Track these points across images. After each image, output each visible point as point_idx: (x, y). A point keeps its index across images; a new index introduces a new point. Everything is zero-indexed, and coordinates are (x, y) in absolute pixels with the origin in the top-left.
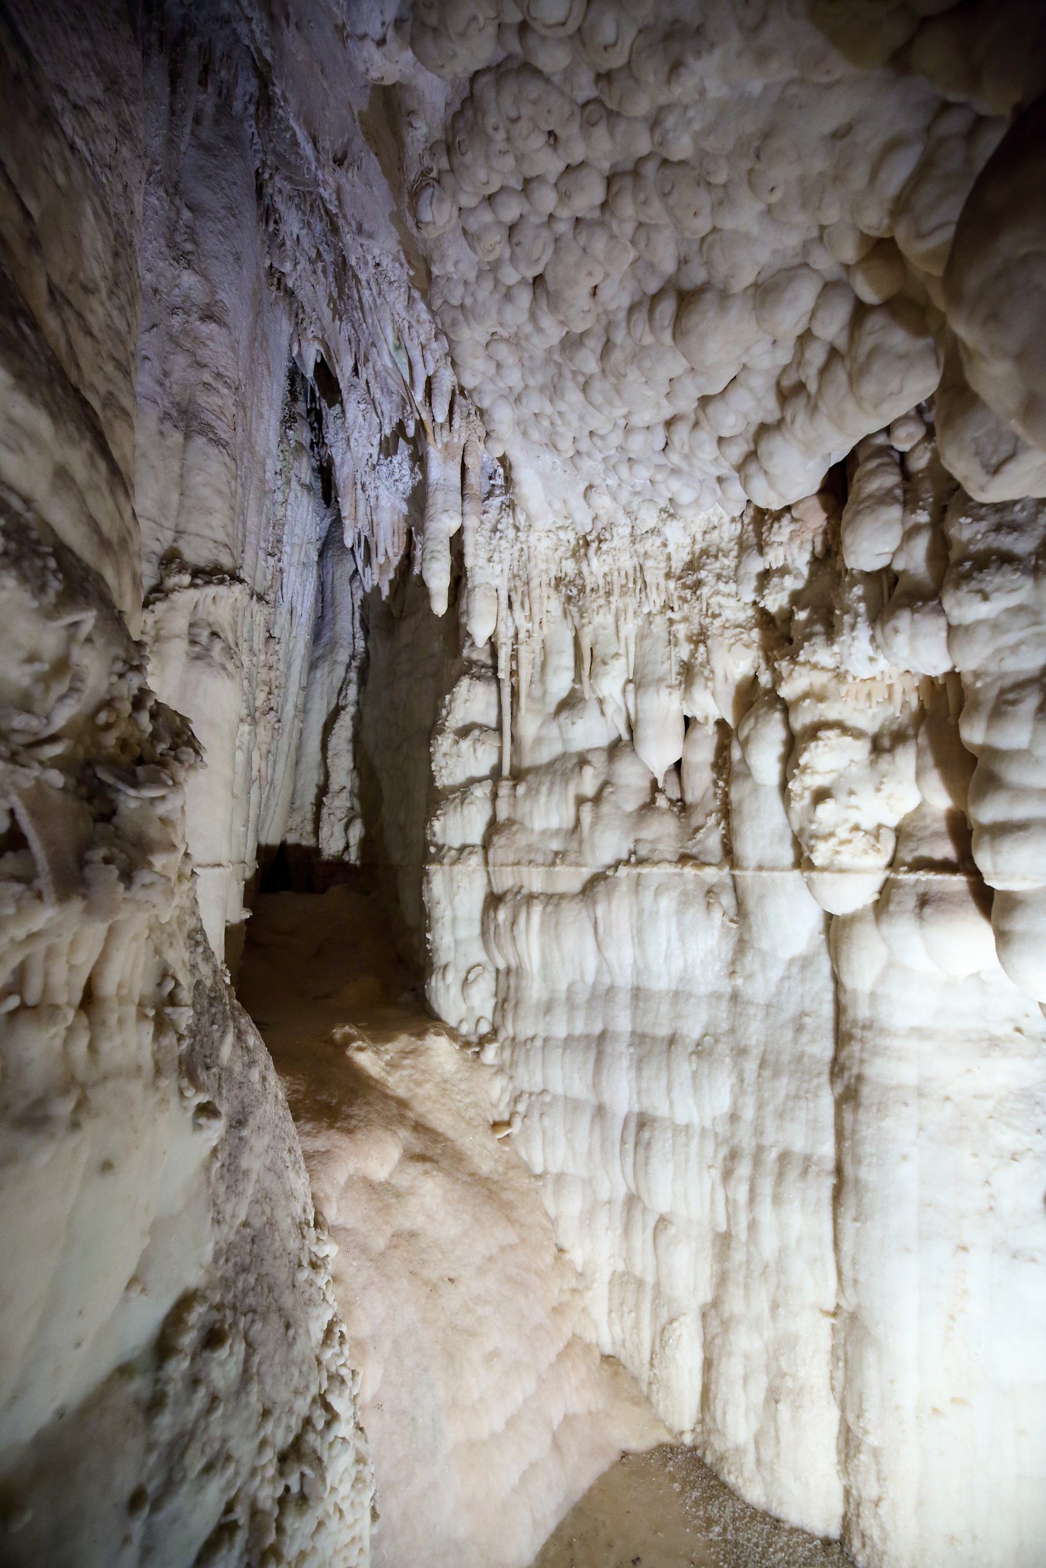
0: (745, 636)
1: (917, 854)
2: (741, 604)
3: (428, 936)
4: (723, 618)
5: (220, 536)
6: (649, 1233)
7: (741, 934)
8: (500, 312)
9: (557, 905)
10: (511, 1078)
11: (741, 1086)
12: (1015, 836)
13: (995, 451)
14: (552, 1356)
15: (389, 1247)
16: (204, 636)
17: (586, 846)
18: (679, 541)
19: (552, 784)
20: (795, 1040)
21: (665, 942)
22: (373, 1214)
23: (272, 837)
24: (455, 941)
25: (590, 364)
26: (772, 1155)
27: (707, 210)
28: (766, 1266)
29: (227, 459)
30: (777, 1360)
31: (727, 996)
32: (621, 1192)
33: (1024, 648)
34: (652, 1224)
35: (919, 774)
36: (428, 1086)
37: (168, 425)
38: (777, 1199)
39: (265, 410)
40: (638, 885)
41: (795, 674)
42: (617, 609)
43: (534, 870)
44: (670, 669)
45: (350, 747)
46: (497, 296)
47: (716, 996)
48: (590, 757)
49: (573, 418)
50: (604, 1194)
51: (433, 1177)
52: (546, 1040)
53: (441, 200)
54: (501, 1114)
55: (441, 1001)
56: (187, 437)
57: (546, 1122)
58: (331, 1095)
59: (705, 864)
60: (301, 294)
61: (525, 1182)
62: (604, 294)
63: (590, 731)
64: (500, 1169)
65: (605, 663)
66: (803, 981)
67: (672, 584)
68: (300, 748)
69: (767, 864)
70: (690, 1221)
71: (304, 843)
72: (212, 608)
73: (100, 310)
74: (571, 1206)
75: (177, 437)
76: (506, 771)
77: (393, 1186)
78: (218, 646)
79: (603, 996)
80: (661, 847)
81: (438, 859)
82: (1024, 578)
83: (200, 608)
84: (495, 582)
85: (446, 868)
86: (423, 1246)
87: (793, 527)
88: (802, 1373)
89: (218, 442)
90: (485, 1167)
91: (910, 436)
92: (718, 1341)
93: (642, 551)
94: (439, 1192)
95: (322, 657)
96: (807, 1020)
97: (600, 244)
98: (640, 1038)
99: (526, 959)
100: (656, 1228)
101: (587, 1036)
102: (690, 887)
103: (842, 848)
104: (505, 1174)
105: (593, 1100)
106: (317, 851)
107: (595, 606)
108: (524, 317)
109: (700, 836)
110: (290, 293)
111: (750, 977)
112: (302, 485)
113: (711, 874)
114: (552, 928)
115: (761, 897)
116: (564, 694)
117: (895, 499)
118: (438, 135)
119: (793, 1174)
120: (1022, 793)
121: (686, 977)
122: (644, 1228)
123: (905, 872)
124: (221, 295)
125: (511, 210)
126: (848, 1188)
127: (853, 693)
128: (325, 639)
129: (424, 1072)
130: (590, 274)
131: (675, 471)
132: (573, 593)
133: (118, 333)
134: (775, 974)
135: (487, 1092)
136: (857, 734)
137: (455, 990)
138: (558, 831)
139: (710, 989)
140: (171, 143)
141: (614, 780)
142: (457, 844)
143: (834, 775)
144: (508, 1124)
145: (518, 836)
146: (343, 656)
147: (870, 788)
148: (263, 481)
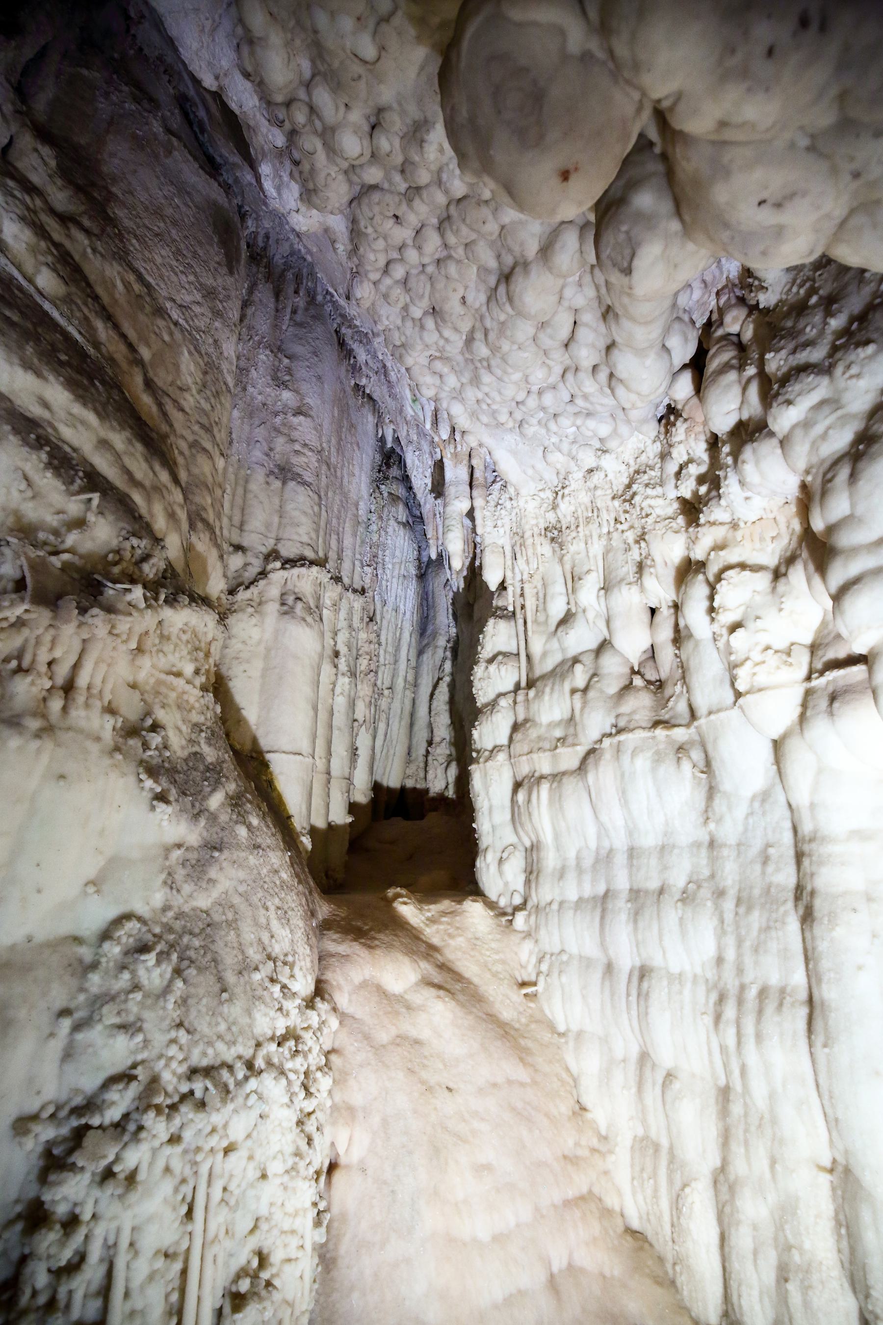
0: (674, 525)
1: (825, 659)
2: (668, 501)
3: (474, 825)
4: (654, 515)
5: (305, 539)
7: (710, 783)
8: (421, 338)
9: (560, 781)
10: (536, 941)
11: (722, 928)
12: (851, 592)
13: (623, 258)
14: (557, 1197)
15: (392, 1043)
16: (290, 600)
17: (579, 728)
18: (615, 470)
19: (553, 684)
20: (763, 873)
22: (381, 1013)
23: (393, 781)
24: (493, 826)
25: (483, 351)
26: (752, 993)
27: (490, 217)
28: (762, 1118)
29: (311, 493)
30: (783, 1230)
31: (706, 843)
32: (634, 1051)
33: (831, 432)
34: (660, 1080)
37: (272, 477)
38: (759, 1037)
40: (618, 751)
41: (699, 535)
42: (586, 536)
43: (541, 754)
44: (630, 569)
45: (447, 707)
46: (417, 329)
47: (697, 845)
48: (581, 658)
49: (494, 394)
50: (619, 1054)
51: (444, 1001)
53: (361, 282)
54: (529, 975)
56: (284, 483)
57: (564, 979)
58: (366, 924)
59: (675, 726)
61: (547, 1036)
62: (469, 299)
63: (580, 639)
64: (523, 1020)
65: (580, 579)
66: (764, 814)
67: (616, 503)
68: (412, 715)
69: (714, 709)
71: (418, 786)
72: (298, 584)
73: (191, 399)
74: (588, 1064)
75: (278, 484)
76: (523, 684)
77: (406, 1000)
78: (299, 605)
79: (604, 859)
80: (637, 717)
82: (819, 378)
83: (289, 582)
84: (500, 542)
85: (481, 765)
86: (426, 1054)
87: (685, 426)
88: (807, 1245)
89: (305, 483)
90: (507, 1015)
92: (727, 1209)
93: (592, 486)
95: (427, 645)
96: (771, 851)
97: (452, 269)
98: (635, 894)
100: (664, 1082)
101: (594, 898)
102: (662, 746)
103: (757, 669)
104: (527, 1025)
105: (604, 961)
106: (427, 791)
107: (569, 538)
108: (436, 335)
109: (671, 704)
110: (370, 397)
111: (719, 821)
112: (399, 523)
113: (680, 734)
114: (556, 800)
115: (715, 740)
116: (561, 615)
117: (732, 367)
118: (350, 247)
120: (855, 551)
122: (654, 1084)
123: (817, 678)
124: (308, 400)
125: (399, 272)
126: (817, 1012)
128: (429, 632)
129: (458, 928)
130: (455, 290)
131: (589, 415)
132: (555, 535)
133: (203, 410)
134: (740, 811)
135: (516, 954)
137: (493, 868)
138: (561, 721)
139: (691, 840)
140: (275, 327)
141: (600, 672)
142: (490, 748)
143: (743, 608)
144: (535, 984)
145: (530, 731)
146: (442, 642)
148: (356, 516)
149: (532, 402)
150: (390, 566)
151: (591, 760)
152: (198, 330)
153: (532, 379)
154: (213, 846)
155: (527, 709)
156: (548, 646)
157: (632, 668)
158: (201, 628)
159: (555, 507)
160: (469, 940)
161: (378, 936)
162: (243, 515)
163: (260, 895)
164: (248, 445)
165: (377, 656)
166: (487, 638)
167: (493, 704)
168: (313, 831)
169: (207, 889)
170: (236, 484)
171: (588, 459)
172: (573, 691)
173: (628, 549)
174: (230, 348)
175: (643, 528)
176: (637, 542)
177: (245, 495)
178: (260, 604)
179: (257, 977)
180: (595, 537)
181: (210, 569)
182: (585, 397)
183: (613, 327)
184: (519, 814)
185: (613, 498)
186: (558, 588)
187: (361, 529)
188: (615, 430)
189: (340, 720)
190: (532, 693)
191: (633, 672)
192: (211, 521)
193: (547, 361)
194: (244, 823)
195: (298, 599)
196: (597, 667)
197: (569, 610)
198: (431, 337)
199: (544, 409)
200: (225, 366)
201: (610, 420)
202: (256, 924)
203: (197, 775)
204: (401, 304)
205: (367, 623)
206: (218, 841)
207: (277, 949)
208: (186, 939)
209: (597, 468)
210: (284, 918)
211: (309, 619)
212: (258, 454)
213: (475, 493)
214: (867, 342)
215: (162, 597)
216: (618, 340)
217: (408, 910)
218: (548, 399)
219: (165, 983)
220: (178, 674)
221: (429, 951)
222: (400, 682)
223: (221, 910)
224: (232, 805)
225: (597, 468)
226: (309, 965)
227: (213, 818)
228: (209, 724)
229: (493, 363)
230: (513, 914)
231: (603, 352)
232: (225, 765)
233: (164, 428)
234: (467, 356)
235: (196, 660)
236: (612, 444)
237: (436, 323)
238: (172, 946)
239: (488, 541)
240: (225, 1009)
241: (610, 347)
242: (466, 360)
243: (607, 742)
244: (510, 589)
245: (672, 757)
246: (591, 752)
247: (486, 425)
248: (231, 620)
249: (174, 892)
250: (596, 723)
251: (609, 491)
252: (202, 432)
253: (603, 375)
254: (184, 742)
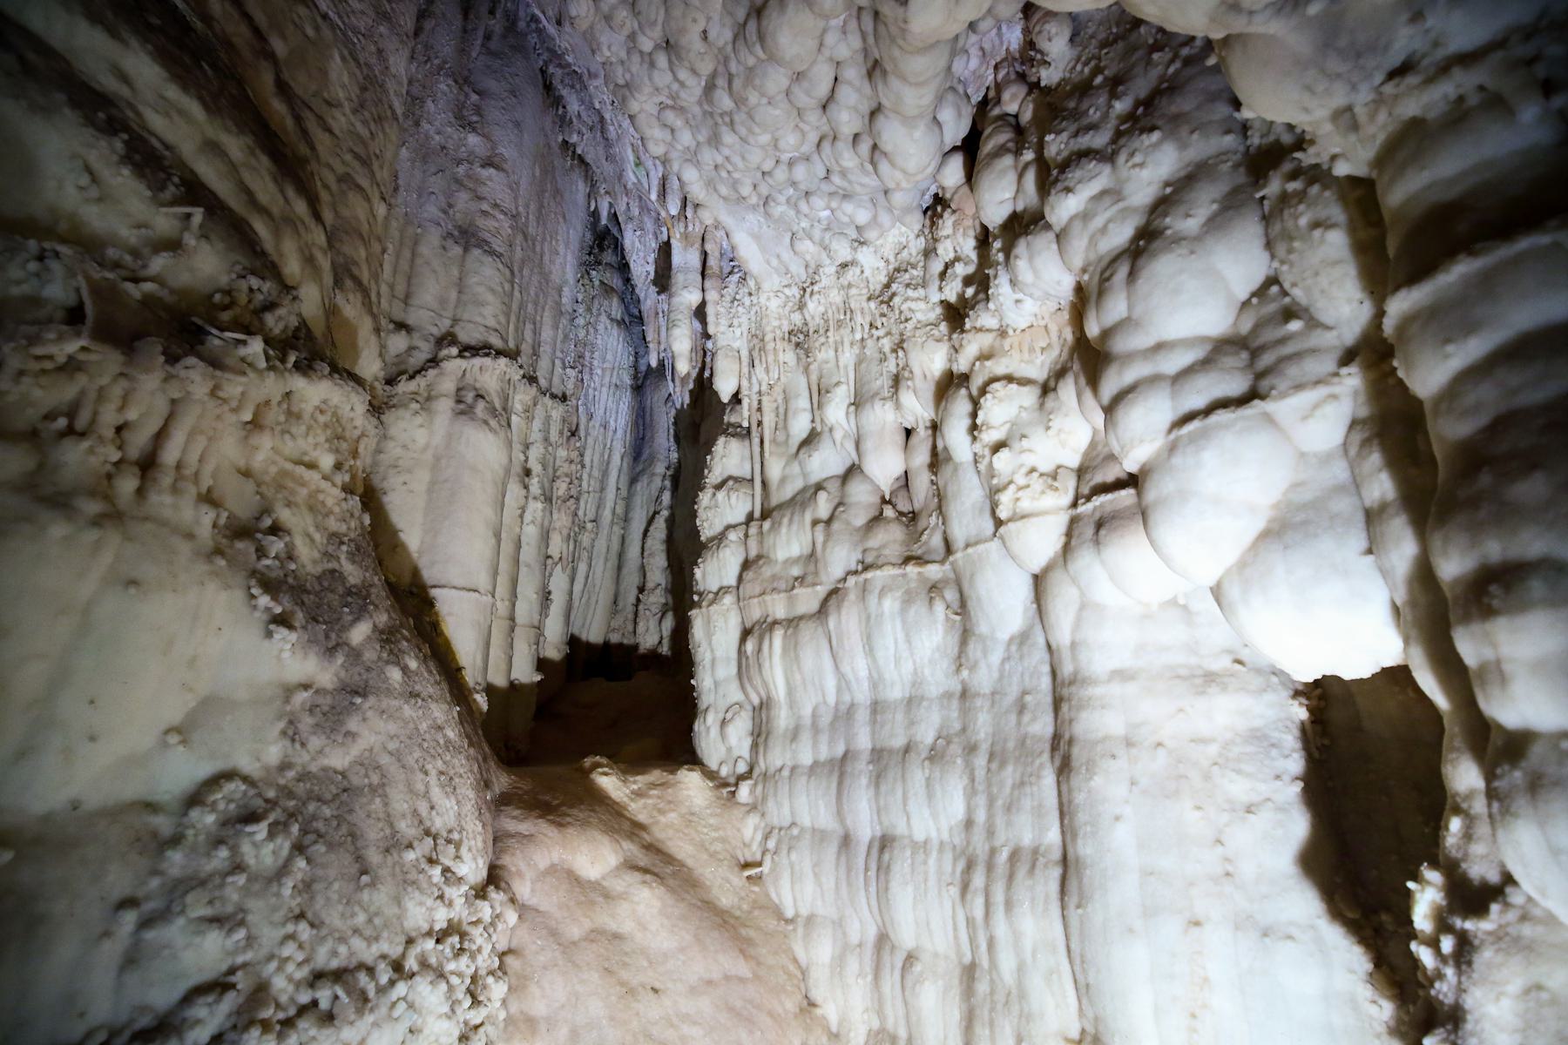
0: (935, 332)
1: (1092, 483)
5: (492, 323)
6: (897, 973)
8: (650, 79)
15: (586, 939)
18: (872, 265)
20: (1019, 723)
21: (896, 648)
22: (572, 903)
23: (594, 634)
25: (726, 103)
26: (1004, 856)
28: (1009, 994)
32: (872, 932)
33: (1111, 226)
34: (899, 965)
35: (1079, 396)
36: (672, 816)
37: (450, 242)
39: (561, 249)
43: (775, 596)
44: (884, 383)
45: (663, 547)
46: (646, 66)
47: (948, 695)
49: (736, 159)
50: (854, 938)
52: (793, 769)
55: (703, 744)
56: (466, 250)
57: (794, 856)
59: (928, 562)
60: (589, 158)
61: (772, 923)
62: (712, 35)
63: (826, 462)
64: (745, 907)
66: (1021, 658)
67: (873, 305)
68: (621, 555)
70: (936, 955)
73: (343, 119)
74: (819, 952)
75: (457, 250)
76: (757, 514)
78: (481, 405)
79: (844, 716)
80: (886, 552)
81: (698, 605)
84: (736, 345)
87: (953, 218)
89: (492, 253)
90: (725, 901)
91: (1014, 96)
94: (657, 904)
95: (643, 471)
96: (1028, 698)
98: (878, 754)
103: (1020, 494)
104: (750, 912)
105: (841, 832)
106: (636, 647)
108: (668, 77)
109: (924, 537)
110: (581, 160)
111: (973, 668)
113: (933, 571)
114: (791, 649)
116: (804, 435)
117: (1009, 151)
119: (1021, 872)
120: (1130, 357)
121: (917, 682)
126: (1071, 871)
127: (1016, 345)
128: (644, 456)
129: (670, 802)
130: (695, 21)
131: (846, 196)
132: (801, 339)
133: (359, 136)
134: (996, 657)
136: (1024, 382)
137: (714, 732)
138: (799, 558)
140: (462, 51)
141: (846, 500)
142: (715, 589)
143: (1008, 426)
144: (760, 864)
146: (660, 468)
147: (1041, 430)
148: (559, 304)
149: (781, 174)
150: (599, 372)
151: (833, 602)
152: (356, 32)
153: (782, 144)
154: (354, 690)
155: (761, 543)
156: (787, 471)
157: (883, 498)
158: (345, 411)
159: (801, 306)
160: (683, 816)
161: (570, 811)
162: (409, 285)
163: (417, 754)
164: (420, 196)
165: (580, 479)
166: (716, 459)
167: (721, 537)
168: (490, 690)
169: (343, 744)
170: (401, 244)
171: (843, 251)
172: (815, 523)
173: (883, 359)
174: (399, 63)
175: (902, 334)
176: (894, 351)
177: (412, 261)
178: (429, 399)
179: (410, 856)
180: (847, 344)
181: (361, 343)
182: (844, 174)
183: (880, 87)
184: (748, 666)
185: (869, 299)
186: (803, 402)
187: (564, 321)
188: (875, 217)
189: (529, 553)
190: (767, 525)
191: (884, 501)
192: (365, 282)
193: (801, 125)
194: (398, 664)
195: (480, 396)
196: (843, 496)
197: (813, 429)
198: (663, 78)
199: (794, 184)
200: (391, 86)
201: (869, 205)
202: (411, 790)
203: (334, 599)
204: (626, 32)
206: (362, 684)
207: (438, 824)
208: (312, 807)
209: (853, 263)
210: (450, 785)
211: (493, 423)
212: (432, 210)
213: (708, 284)
214: (1152, 129)
215: (292, 359)
216: (885, 102)
217: (609, 782)
218: (800, 172)
219: (281, 862)
220: (312, 466)
221: (635, 829)
222: (607, 514)
223: (363, 771)
224: (382, 640)
225: (853, 263)
226: (480, 844)
227: (355, 654)
228: (352, 535)
229: (736, 118)
230: (736, 785)
231: (867, 120)
232: (373, 590)
233: (303, 150)
234: (706, 107)
235: (337, 451)
236: (871, 235)
237: (670, 61)
238: (292, 815)
239: (722, 341)
240: (365, 896)
241: (874, 114)
242: (705, 113)
243: (852, 581)
244: (745, 402)
245: (924, 596)
246: (834, 592)
247: (724, 198)
248: (388, 417)
249: (298, 746)
250: (840, 559)
251: (865, 291)
252: (356, 164)
253: (865, 147)
254: (316, 555)
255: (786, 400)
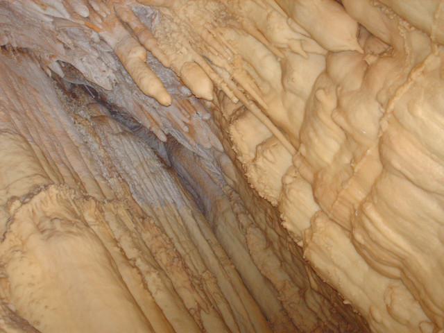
3: (346, 302)
16: (47, 224)
29: (11, 136)
60: (24, 45)
63: (305, 74)
68: (245, 284)
84: (190, 58)
99: (397, 249)
110: (21, 51)
112: (117, 135)
116: (279, 73)
138: (341, 149)
150: (134, 172)
184: (369, 252)
205: (143, 223)
211: (74, 229)
222: (212, 261)
255: (249, 63)
